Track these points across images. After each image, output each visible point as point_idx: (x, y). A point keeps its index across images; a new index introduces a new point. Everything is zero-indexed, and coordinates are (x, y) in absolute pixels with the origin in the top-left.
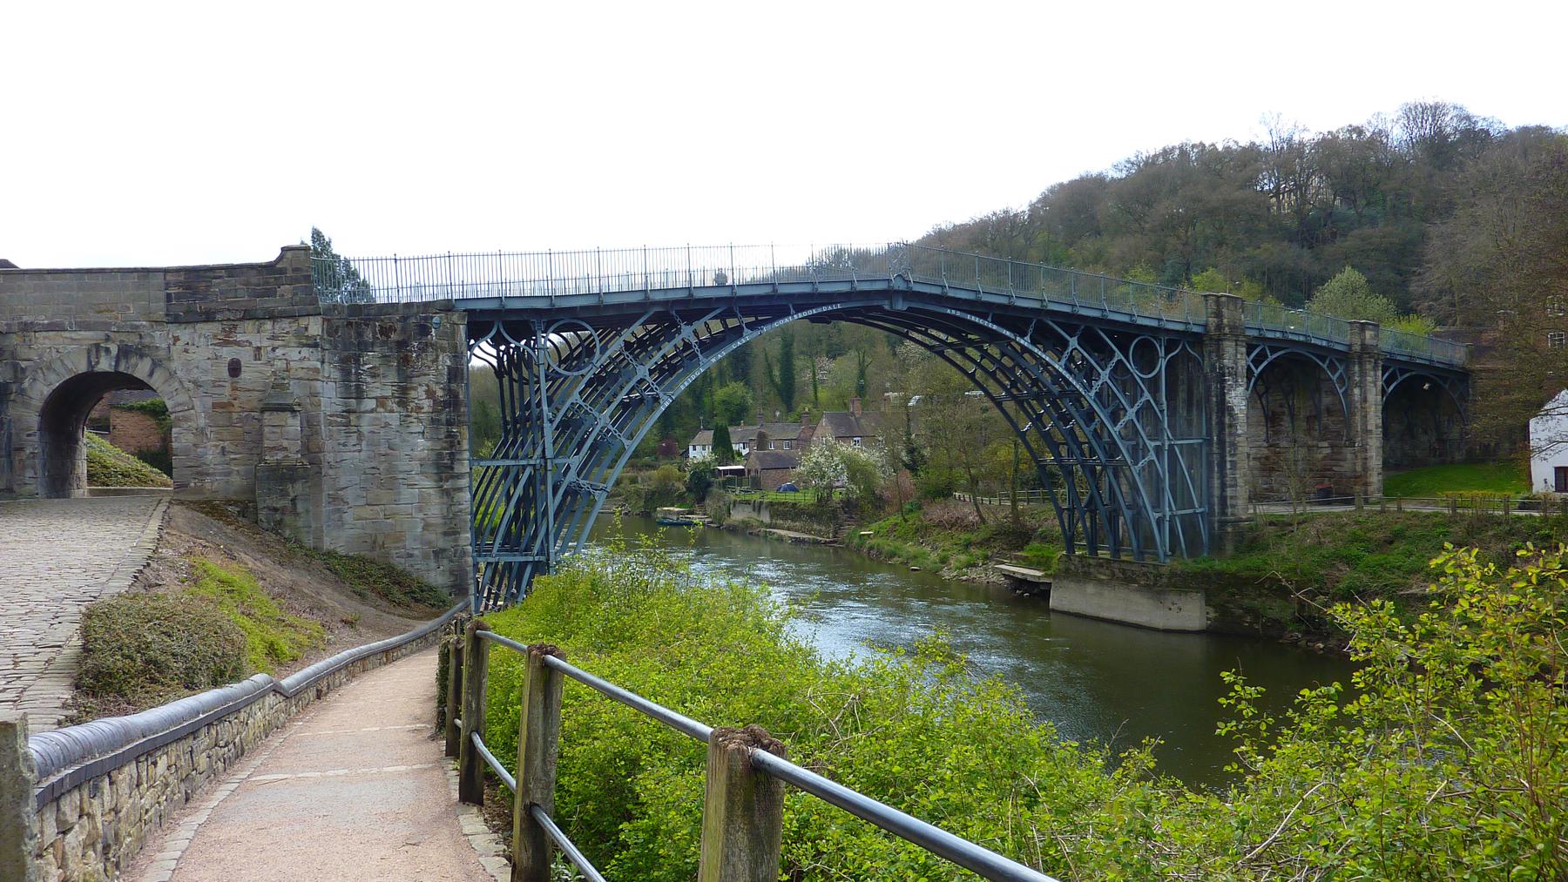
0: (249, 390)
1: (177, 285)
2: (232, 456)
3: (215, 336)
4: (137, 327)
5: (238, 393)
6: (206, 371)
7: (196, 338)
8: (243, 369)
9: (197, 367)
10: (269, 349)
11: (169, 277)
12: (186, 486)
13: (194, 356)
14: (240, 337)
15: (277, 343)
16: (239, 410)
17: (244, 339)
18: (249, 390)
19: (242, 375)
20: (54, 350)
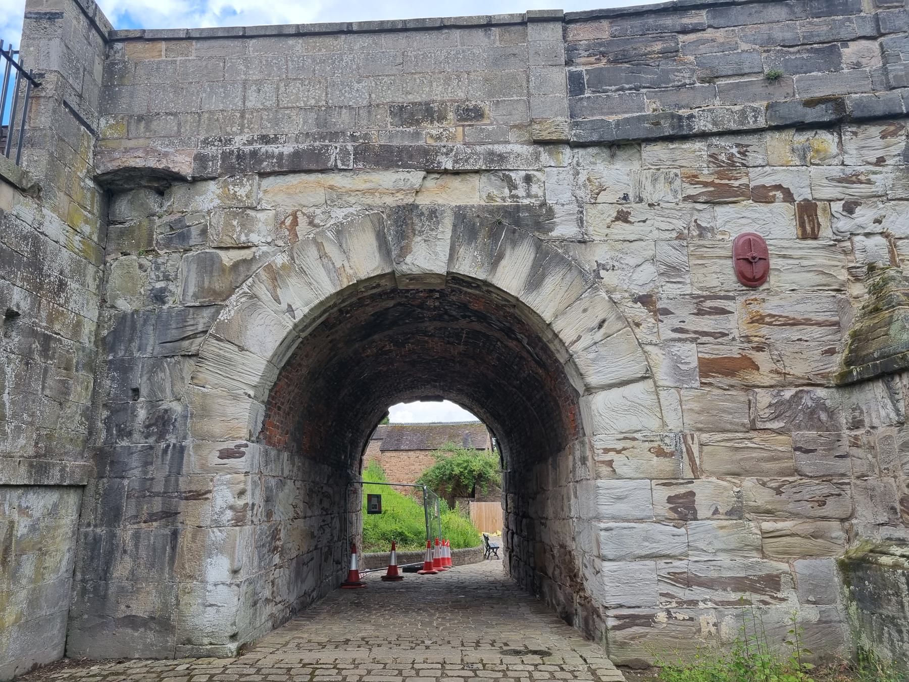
0: (795, 323)
1: (598, 50)
2: (768, 526)
3: (693, 179)
4: (502, 158)
5: (765, 330)
6: (672, 271)
7: (648, 185)
8: (774, 263)
9: (653, 260)
10: (837, 207)
11: (583, 34)
12: (648, 620)
13: (645, 227)
14: (757, 178)
15: (858, 190)
16: (775, 379)
17: (769, 181)
18: (795, 323)
19: (773, 280)
20: (302, 221)
